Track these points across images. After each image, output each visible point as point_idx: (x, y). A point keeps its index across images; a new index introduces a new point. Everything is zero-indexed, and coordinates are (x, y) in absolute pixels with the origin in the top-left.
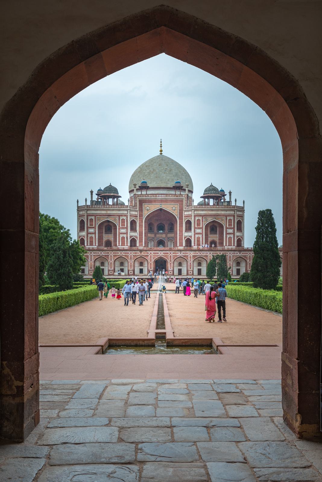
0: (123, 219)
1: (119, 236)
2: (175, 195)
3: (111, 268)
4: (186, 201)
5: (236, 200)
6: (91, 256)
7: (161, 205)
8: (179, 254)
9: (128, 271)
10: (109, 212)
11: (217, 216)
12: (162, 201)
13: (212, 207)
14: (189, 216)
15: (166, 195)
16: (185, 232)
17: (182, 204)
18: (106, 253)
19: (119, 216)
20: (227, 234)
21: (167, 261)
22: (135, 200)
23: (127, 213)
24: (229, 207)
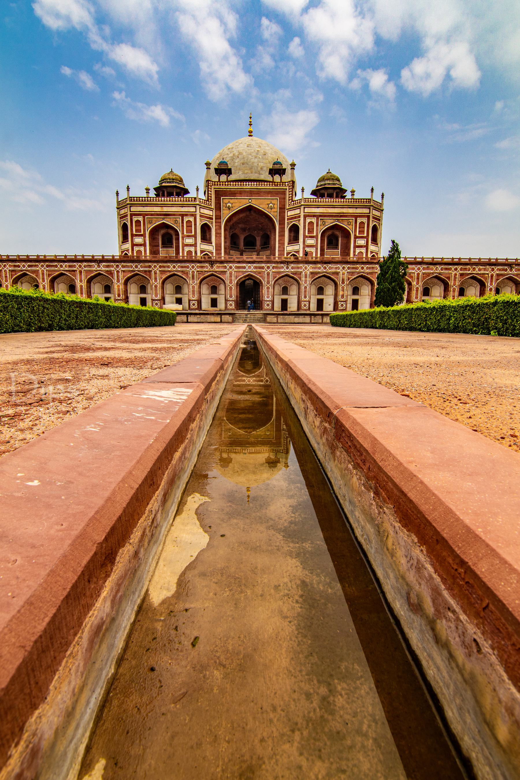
0: (189, 222)
1: (183, 250)
3: (156, 296)
6: (118, 272)
8: (285, 270)
9: (189, 301)
10: (165, 209)
11: (341, 216)
12: (251, 193)
14: (295, 218)
16: (289, 244)
17: (285, 198)
18: (146, 267)
19: (183, 216)
20: (356, 247)
21: (262, 283)
22: (208, 191)
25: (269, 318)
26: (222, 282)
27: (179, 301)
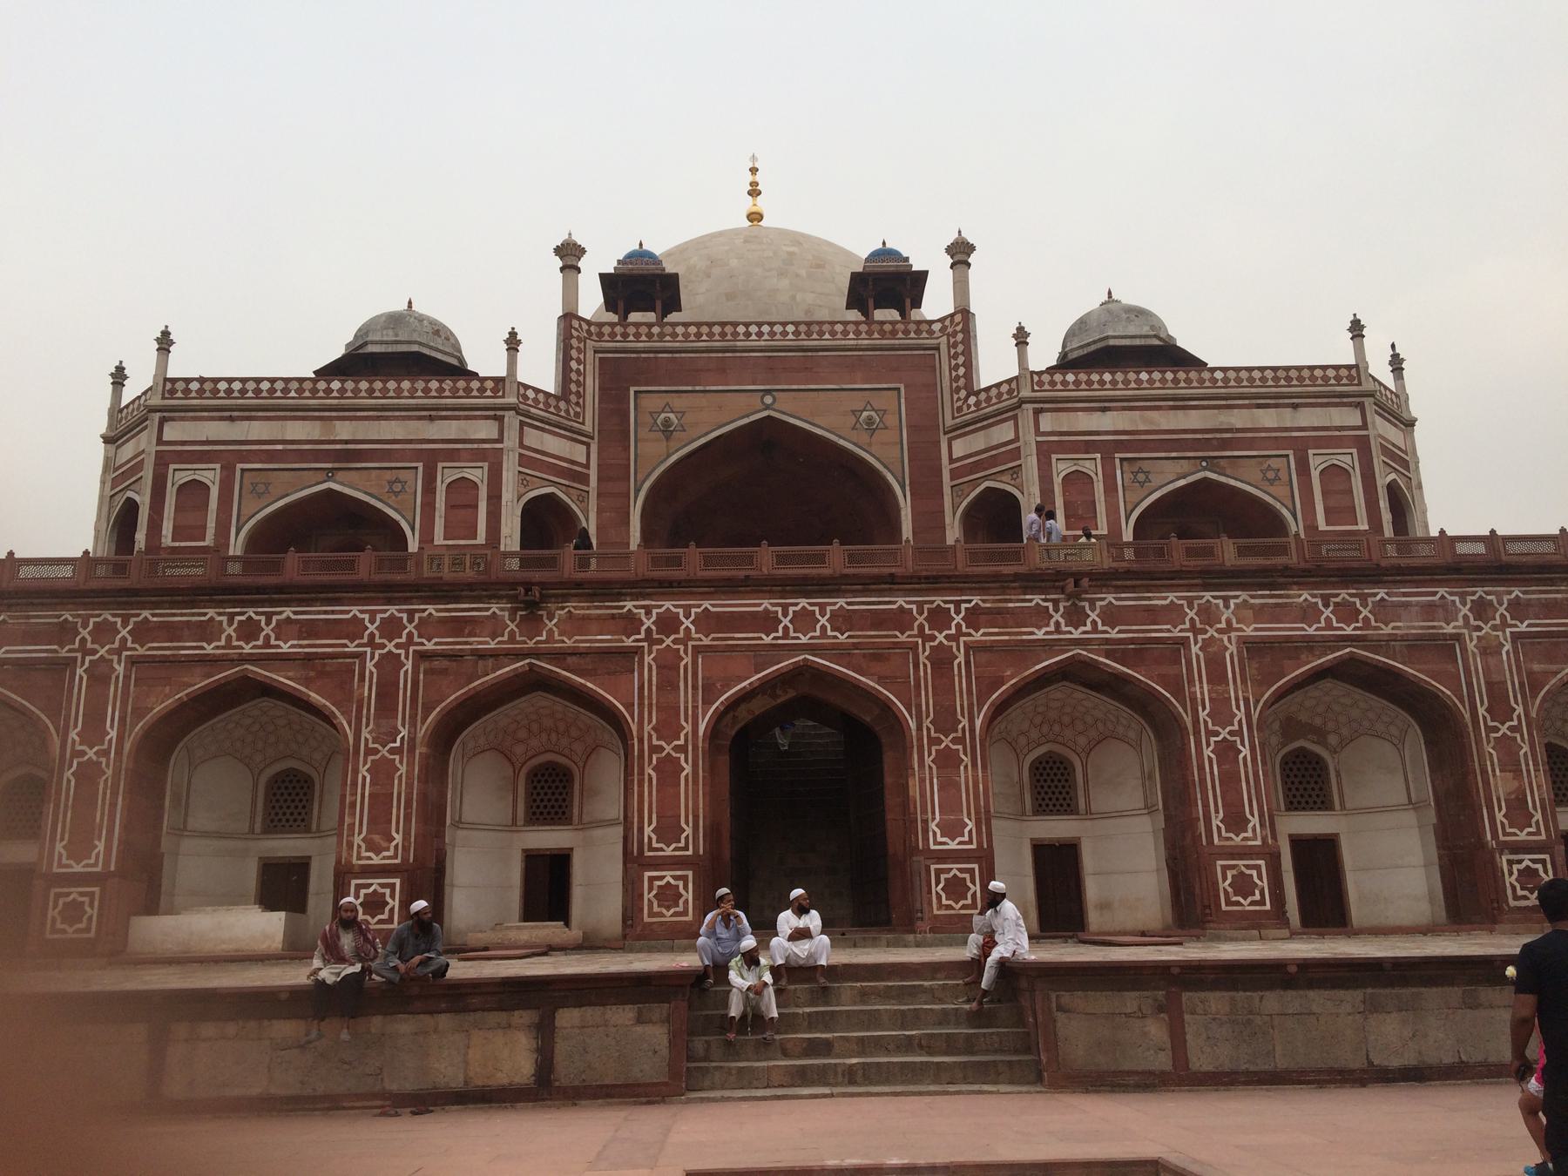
2: (876, 327)
3: (79, 849)
4: (961, 360)
5: (1357, 329)
7: (768, 392)
8: (1055, 630)
10: (344, 430)
11: (1225, 444)
13: (1176, 381)
14: (993, 461)
15: (803, 328)
17: (932, 387)
18: (32, 636)
19: (431, 458)
21: (896, 724)
23: (495, 436)
24: (1313, 378)
25: (1078, 1028)
26: (608, 734)
27: (282, 886)
